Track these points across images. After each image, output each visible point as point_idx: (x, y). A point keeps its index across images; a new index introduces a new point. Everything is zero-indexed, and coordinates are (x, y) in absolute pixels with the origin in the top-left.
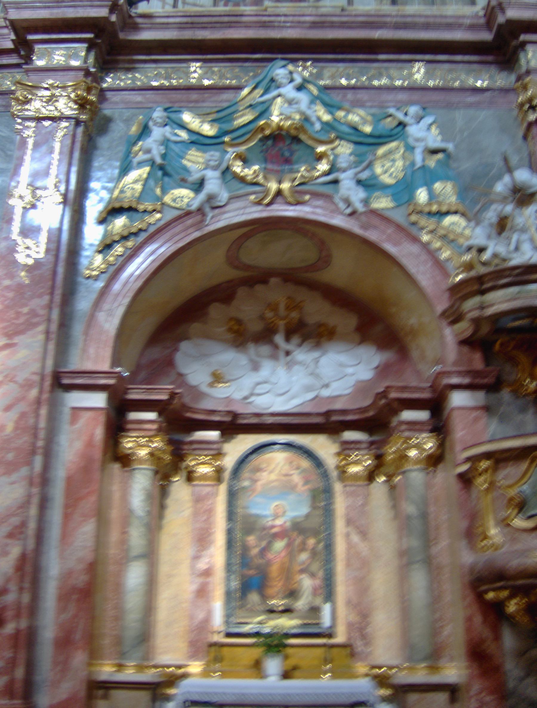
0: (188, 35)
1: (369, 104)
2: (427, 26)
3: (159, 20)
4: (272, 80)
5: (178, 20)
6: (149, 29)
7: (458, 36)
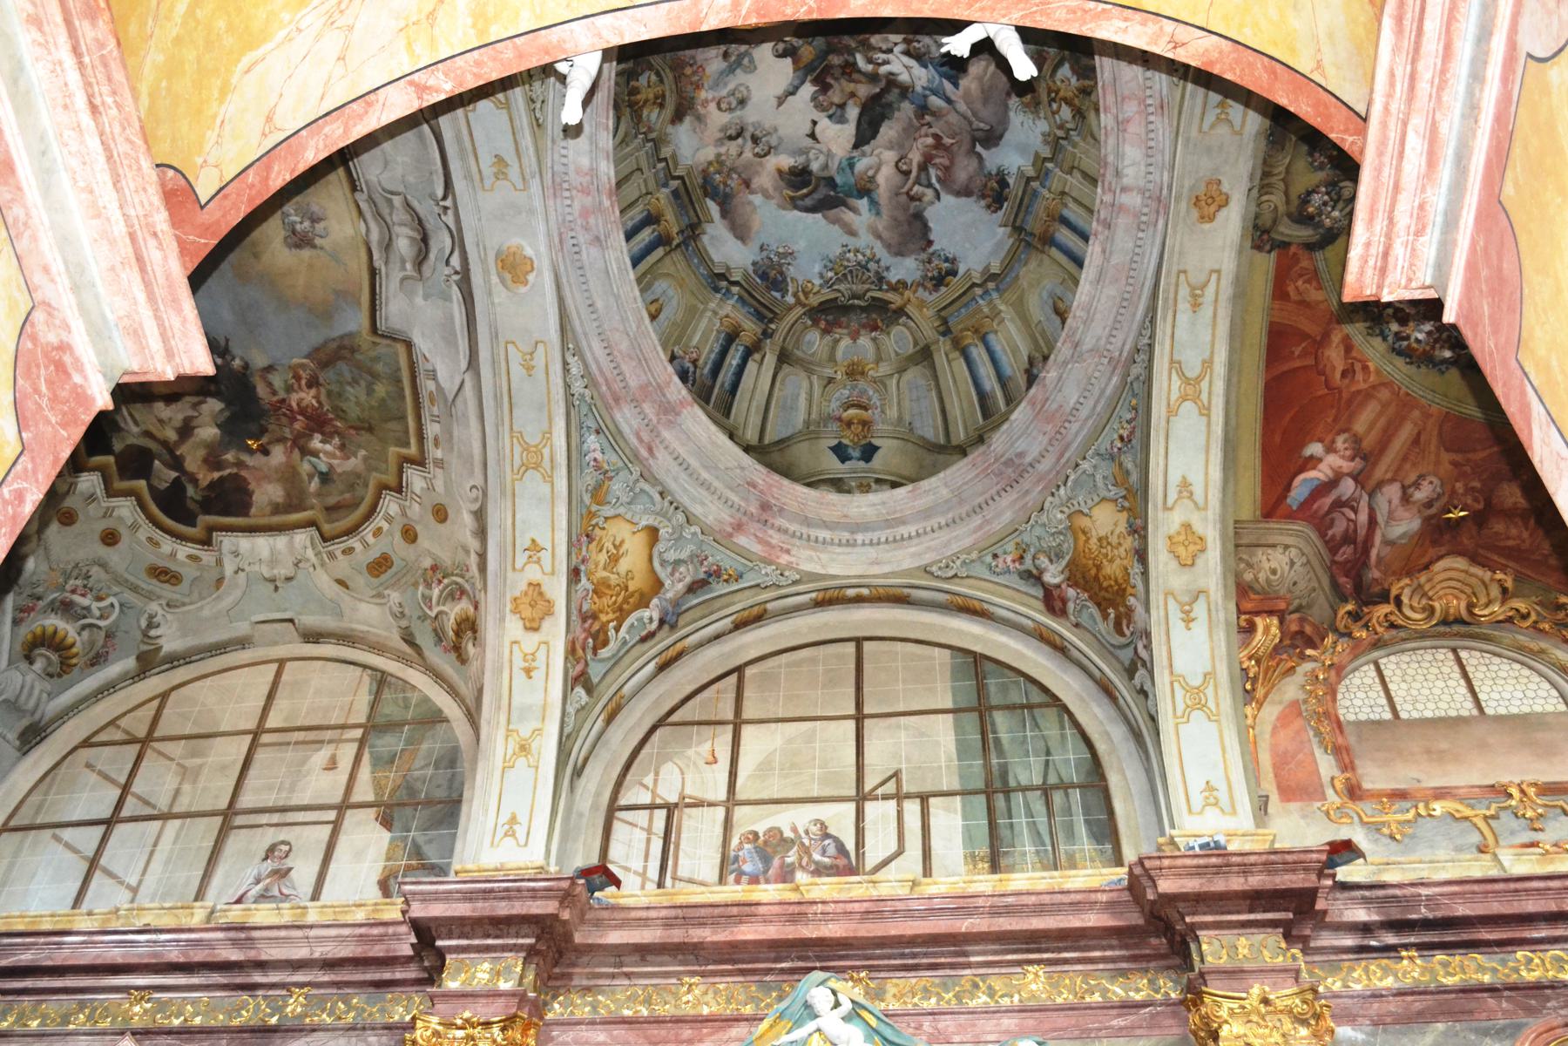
0: (677, 935)
1: (957, 1038)
2: (1040, 910)
3: (633, 914)
4: (807, 1006)
5: (664, 913)
6: (617, 927)
7: (1092, 920)
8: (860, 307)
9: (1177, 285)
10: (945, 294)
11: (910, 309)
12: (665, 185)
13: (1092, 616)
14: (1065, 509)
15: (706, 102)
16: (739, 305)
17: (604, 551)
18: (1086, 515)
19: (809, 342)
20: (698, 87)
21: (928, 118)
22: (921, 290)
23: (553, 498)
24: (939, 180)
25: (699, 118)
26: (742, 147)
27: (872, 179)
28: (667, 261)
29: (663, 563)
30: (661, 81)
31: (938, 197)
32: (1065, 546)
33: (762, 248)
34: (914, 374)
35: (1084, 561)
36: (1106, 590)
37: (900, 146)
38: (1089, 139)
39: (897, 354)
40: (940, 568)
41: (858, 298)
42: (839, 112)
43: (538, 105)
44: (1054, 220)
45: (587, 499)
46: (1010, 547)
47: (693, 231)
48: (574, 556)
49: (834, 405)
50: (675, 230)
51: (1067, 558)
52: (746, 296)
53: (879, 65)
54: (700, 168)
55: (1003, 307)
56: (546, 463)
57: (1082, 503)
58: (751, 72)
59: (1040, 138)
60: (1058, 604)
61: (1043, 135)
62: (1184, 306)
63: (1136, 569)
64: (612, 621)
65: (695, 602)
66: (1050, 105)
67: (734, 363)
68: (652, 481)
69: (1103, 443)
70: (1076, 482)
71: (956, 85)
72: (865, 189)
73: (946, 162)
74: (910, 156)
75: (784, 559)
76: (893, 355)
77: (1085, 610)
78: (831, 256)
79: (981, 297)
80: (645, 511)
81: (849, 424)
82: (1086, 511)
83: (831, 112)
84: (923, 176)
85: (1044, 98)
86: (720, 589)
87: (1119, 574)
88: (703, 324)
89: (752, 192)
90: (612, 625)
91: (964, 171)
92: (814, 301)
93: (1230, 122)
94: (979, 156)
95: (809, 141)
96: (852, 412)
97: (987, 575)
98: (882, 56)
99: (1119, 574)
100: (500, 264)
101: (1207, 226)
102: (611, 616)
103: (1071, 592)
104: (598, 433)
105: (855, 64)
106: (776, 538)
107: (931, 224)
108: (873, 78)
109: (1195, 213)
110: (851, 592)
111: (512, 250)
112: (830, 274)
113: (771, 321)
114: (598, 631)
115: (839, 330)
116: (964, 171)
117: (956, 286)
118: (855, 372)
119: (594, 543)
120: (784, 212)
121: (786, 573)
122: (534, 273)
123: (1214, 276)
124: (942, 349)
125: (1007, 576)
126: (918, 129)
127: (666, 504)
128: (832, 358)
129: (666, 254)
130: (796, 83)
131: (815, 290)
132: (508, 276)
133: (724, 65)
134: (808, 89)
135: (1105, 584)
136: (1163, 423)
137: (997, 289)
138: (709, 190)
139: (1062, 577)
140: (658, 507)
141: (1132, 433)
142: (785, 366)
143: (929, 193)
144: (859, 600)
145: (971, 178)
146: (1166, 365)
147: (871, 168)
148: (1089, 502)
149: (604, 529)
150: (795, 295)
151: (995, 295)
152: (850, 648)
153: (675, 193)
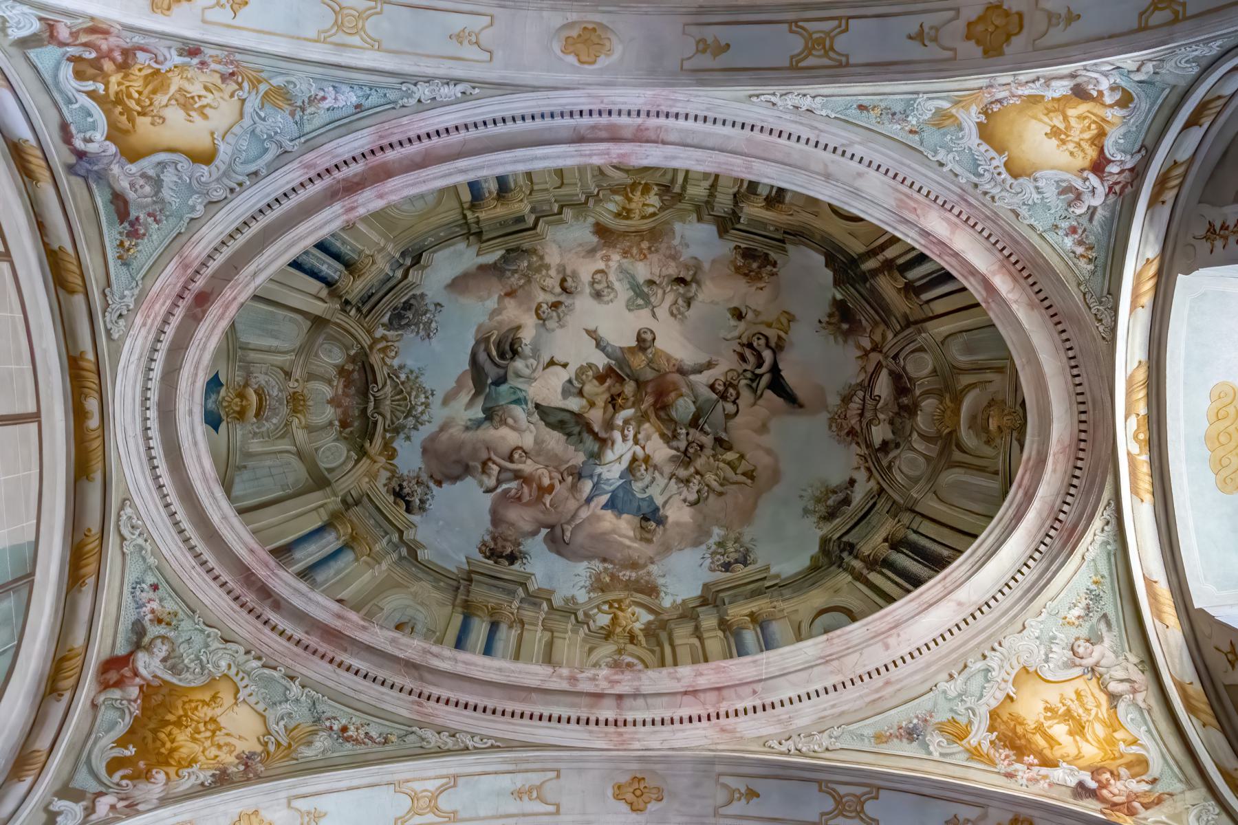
8: (365, 409)
9: (543, 770)
10: (386, 500)
11: (365, 463)
12: (533, 210)
13: (113, 725)
14: (234, 670)
15: (607, 259)
16: (381, 277)
17: (203, 92)
18: (236, 699)
19: (330, 351)
20: (626, 253)
21: (571, 478)
22: (388, 474)
23: (298, 38)
24: (506, 491)
25: (592, 252)
26: (551, 292)
27: (503, 422)
28: (455, 204)
29: (162, 165)
30: (644, 217)
31: (488, 491)
32: (189, 676)
33: (438, 305)
34: (297, 472)
35: (179, 703)
36: (155, 739)
37: (539, 450)
38: (587, 648)
39: (317, 450)
40: (130, 518)
41: (376, 407)
42: (575, 391)
43: (773, 99)
44: (491, 616)
45: (278, 81)
46: (170, 605)
47: (475, 234)
48: (213, 52)
49: (262, 379)
50: (483, 215)
51: (175, 680)
52: (390, 285)
53: (622, 432)
54: (539, 247)
55: (384, 566)
56: (341, 38)
57: (248, 691)
58: (627, 306)
59: (569, 595)
60: (113, 676)
61: (573, 597)
62: (520, 781)
63: (205, 776)
64: (106, 89)
65: (99, 202)
66: (605, 603)
67: (324, 268)
68: (275, 165)
69: (327, 708)
70: (272, 679)
71: (605, 507)
72: (491, 415)
73: (526, 498)
74: (529, 462)
75: (139, 320)
76: (318, 444)
77: (118, 713)
78: (422, 379)
79: (390, 541)
80: (237, 151)
81: (242, 396)
82: (241, 696)
83: (575, 382)
84: (510, 475)
85: (611, 596)
86: (112, 235)
87: (184, 752)
88: (374, 237)
89: (501, 298)
90: (101, 88)
91: (520, 517)
92: (375, 359)
93: (730, 802)
94: (534, 533)
95: (546, 359)
96: (254, 398)
97: (130, 578)
98: (630, 433)
99: (184, 752)
100: (590, 26)
101: (610, 793)
102: (114, 88)
103: (134, 692)
104: (358, 106)
105: (623, 408)
106: (160, 309)
107: (458, 484)
108: (609, 425)
109: (624, 779)
110: (92, 404)
111: (607, 43)
112: (403, 377)
113: (359, 310)
114: (101, 69)
115: (341, 386)
116: (520, 517)
117: (397, 513)
118: (296, 402)
119: (219, 82)
120: (473, 330)
121: (122, 322)
122: (576, 63)
123: (552, 809)
124: (328, 501)
125: (133, 605)
126: (556, 468)
127: (240, 178)
128: (311, 377)
129: (461, 203)
130: (609, 349)
131: (388, 361)
132: (574, 33)
133: (641, 281)
134: (601, 361)
135: (162, 736)
136: (388, 778)
137: (401, 558)
138: (513, 254)
139: (150, 677)
140: (239, 168)
141: (357, 741)
142: (309, 323)
143: (491, 482)
144: (78, 414)
145: (513, 525)
146: (452, 771)
147: (515, 421)
148: (252, 700)
149: (232, 96)
150: (384, 338)
151: (395, 556)
152: (31, 408)
153: (521, 219)
